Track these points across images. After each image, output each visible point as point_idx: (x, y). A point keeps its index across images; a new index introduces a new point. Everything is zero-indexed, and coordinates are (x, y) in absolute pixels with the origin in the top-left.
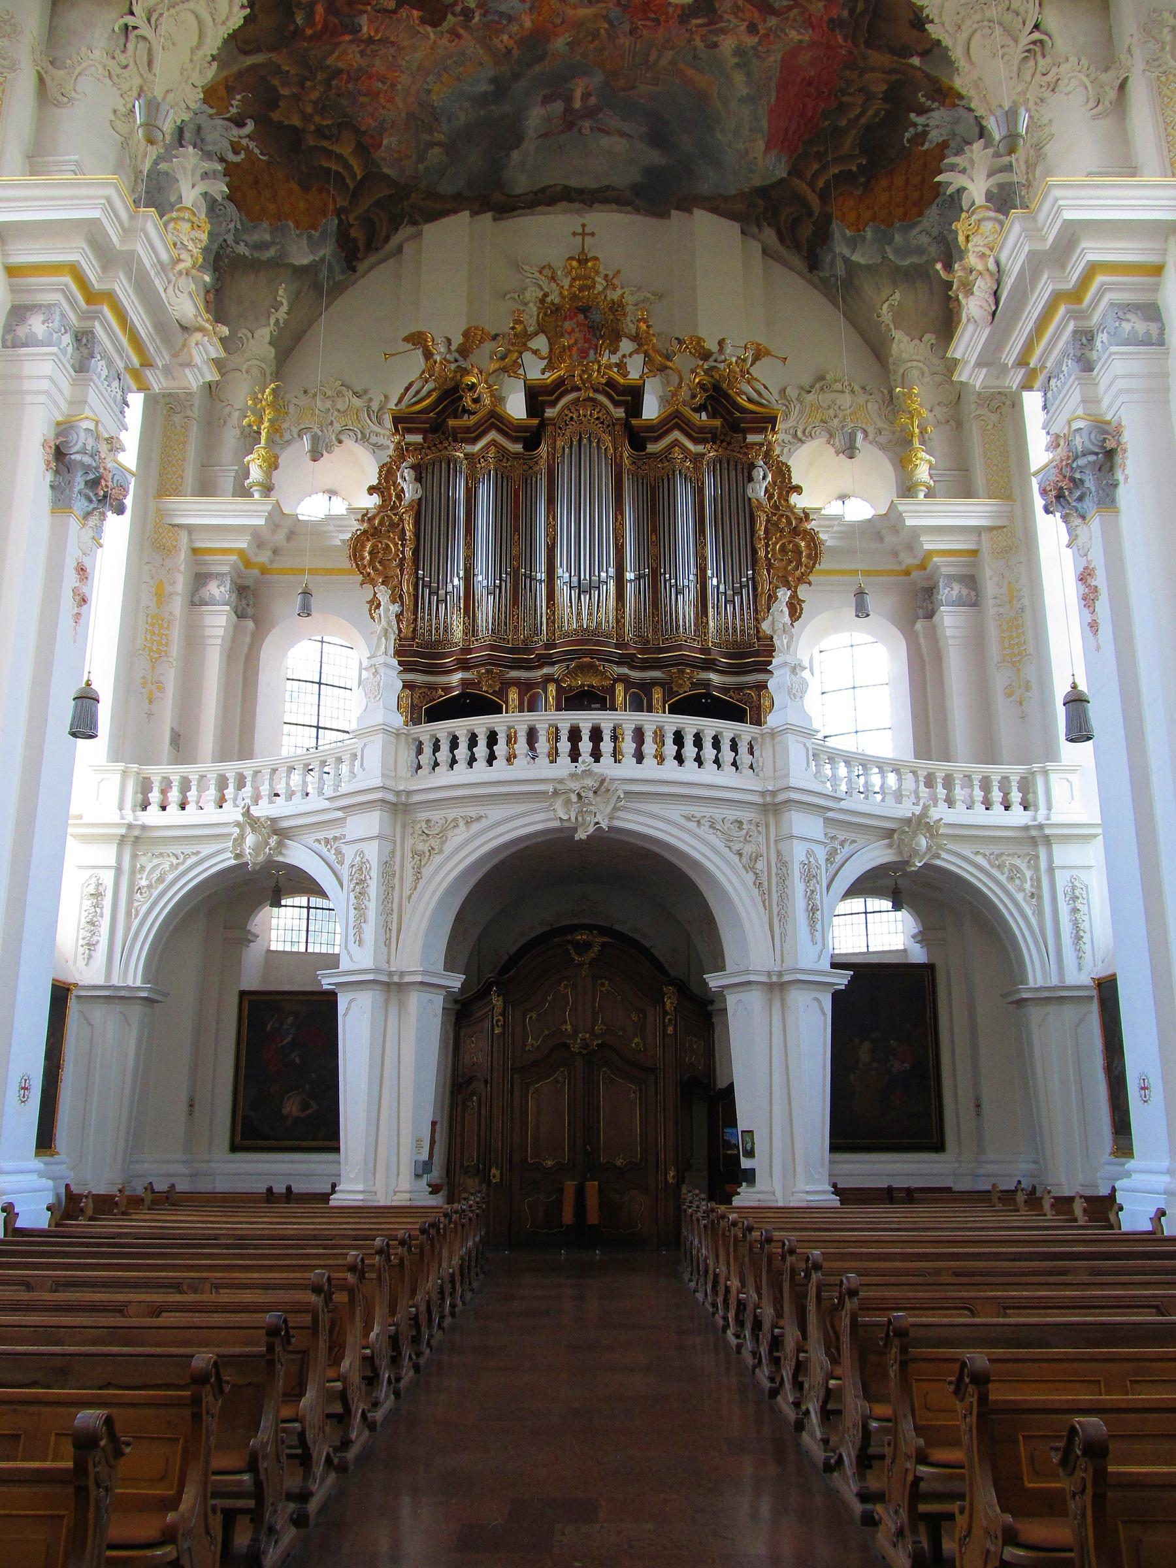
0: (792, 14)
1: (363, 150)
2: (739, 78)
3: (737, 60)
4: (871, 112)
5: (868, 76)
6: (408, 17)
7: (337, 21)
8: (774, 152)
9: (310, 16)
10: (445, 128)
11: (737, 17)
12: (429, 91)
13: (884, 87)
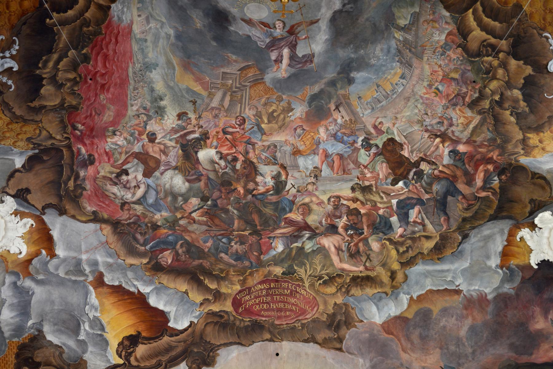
0: (123, 157)
1: (463, 32)
2: (160, 87)
3: (163, 103)
4: (51, 64)
5: (57, 101)
6: (412, 152)
7: (467, 166)
8: (124, 24)
9: (487, 180)
10: (393, 43)
11: (164, 144)
12: (403, 77)
13: (43, 91)
